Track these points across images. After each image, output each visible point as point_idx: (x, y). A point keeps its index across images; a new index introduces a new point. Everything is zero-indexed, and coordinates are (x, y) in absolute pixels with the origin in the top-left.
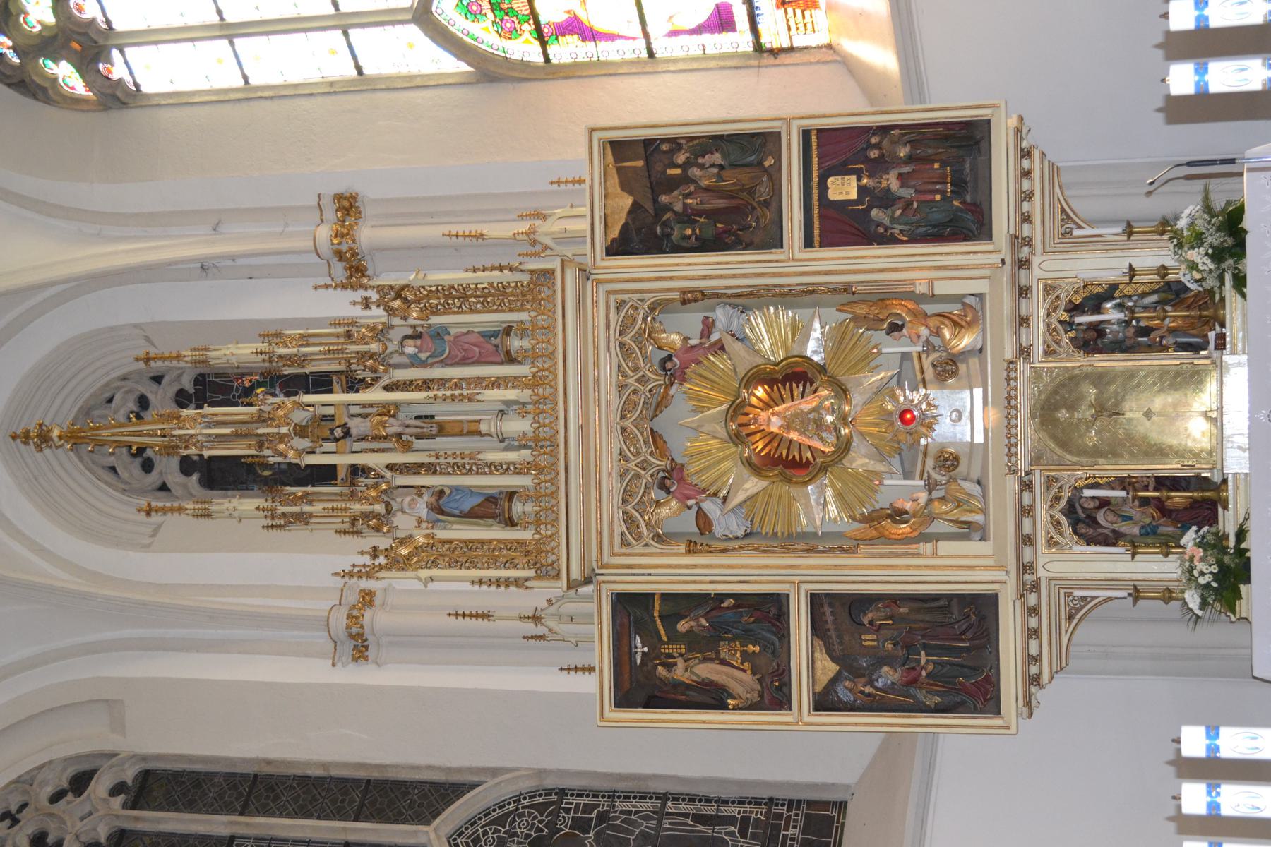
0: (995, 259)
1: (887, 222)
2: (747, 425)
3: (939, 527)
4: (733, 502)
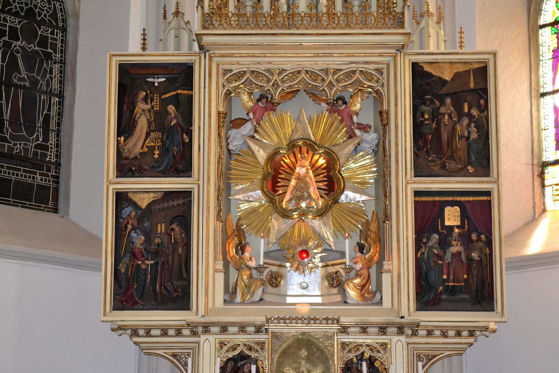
0: (404, 312)
1: (430, 244)
2: (301, 152)
3: (233, 275)
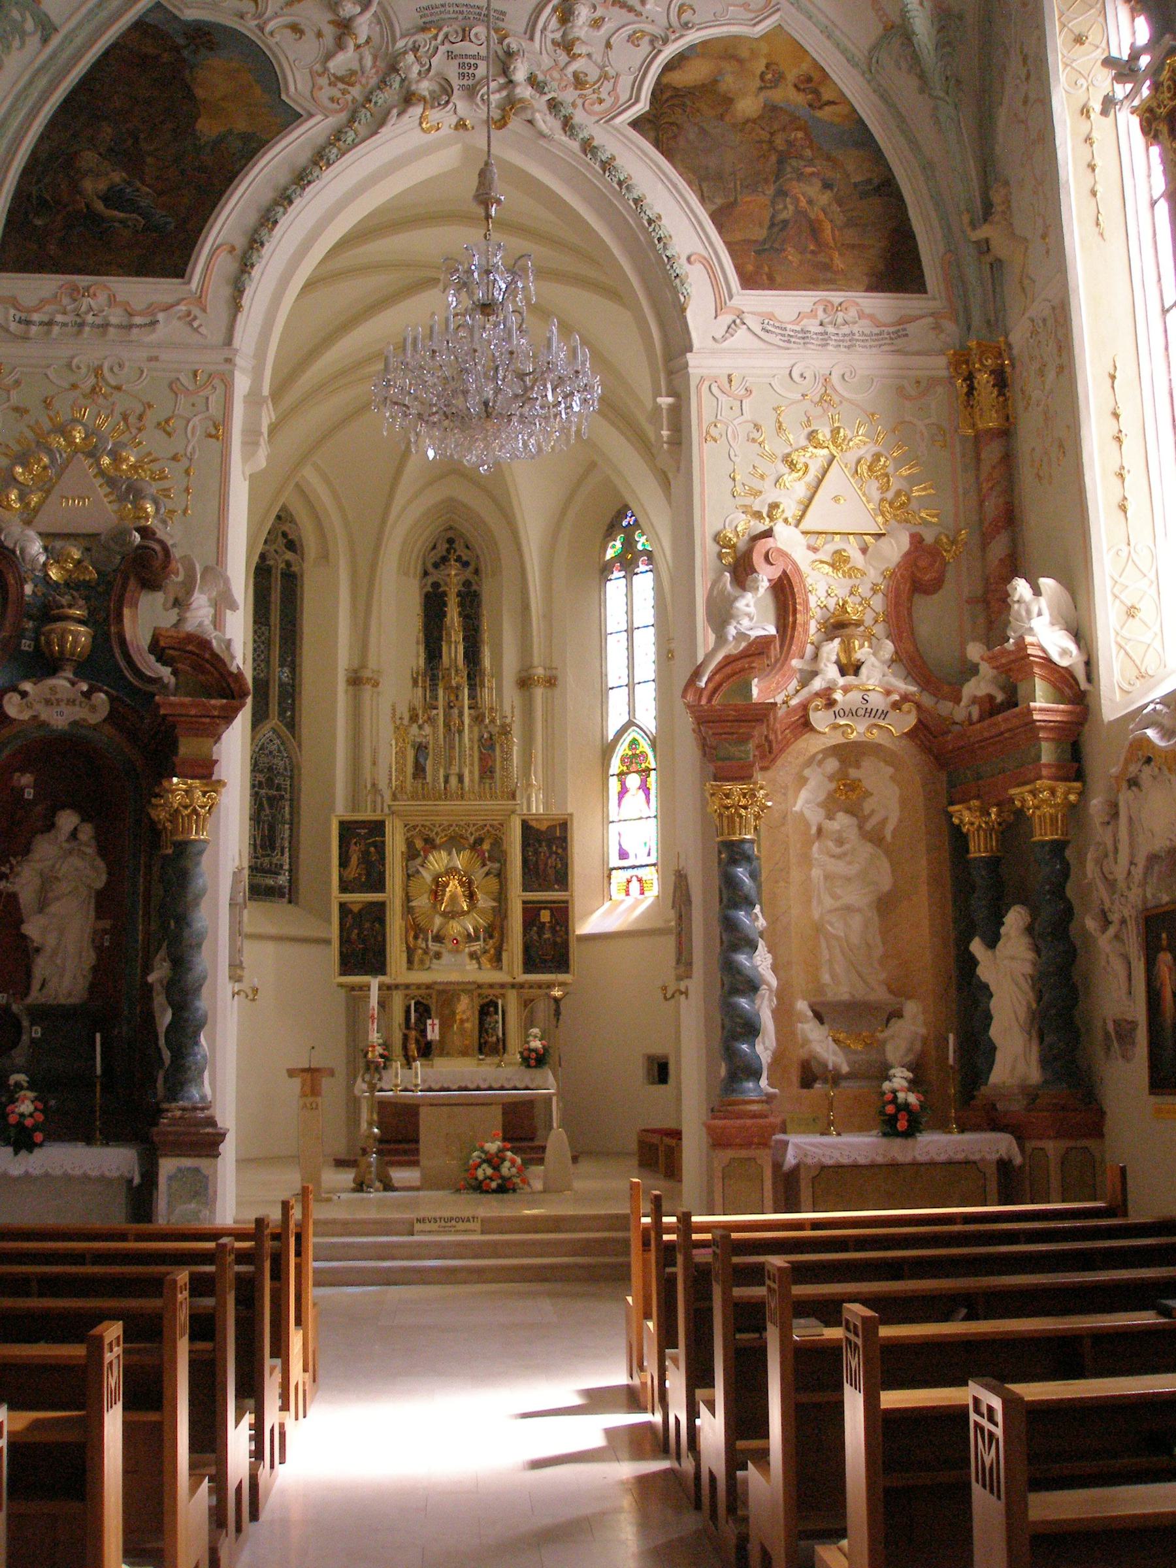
4: (421, 869)
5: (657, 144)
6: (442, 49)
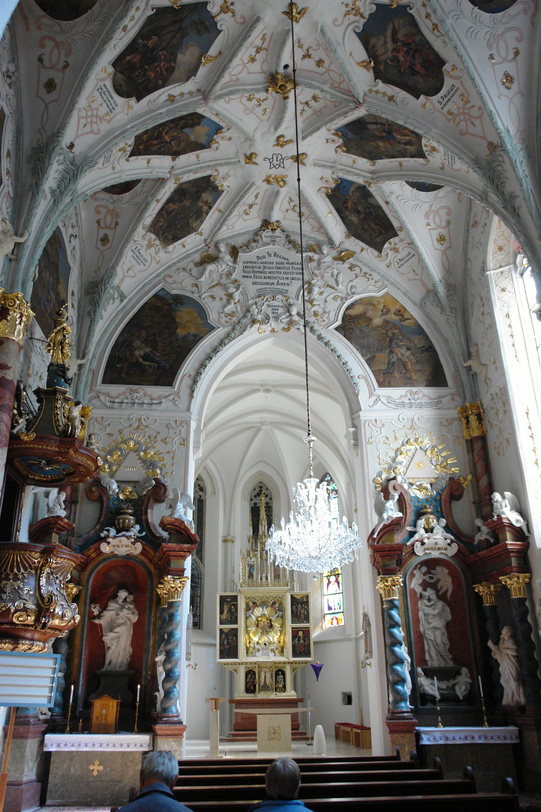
5: (345, 336)
6: (265, 304)
